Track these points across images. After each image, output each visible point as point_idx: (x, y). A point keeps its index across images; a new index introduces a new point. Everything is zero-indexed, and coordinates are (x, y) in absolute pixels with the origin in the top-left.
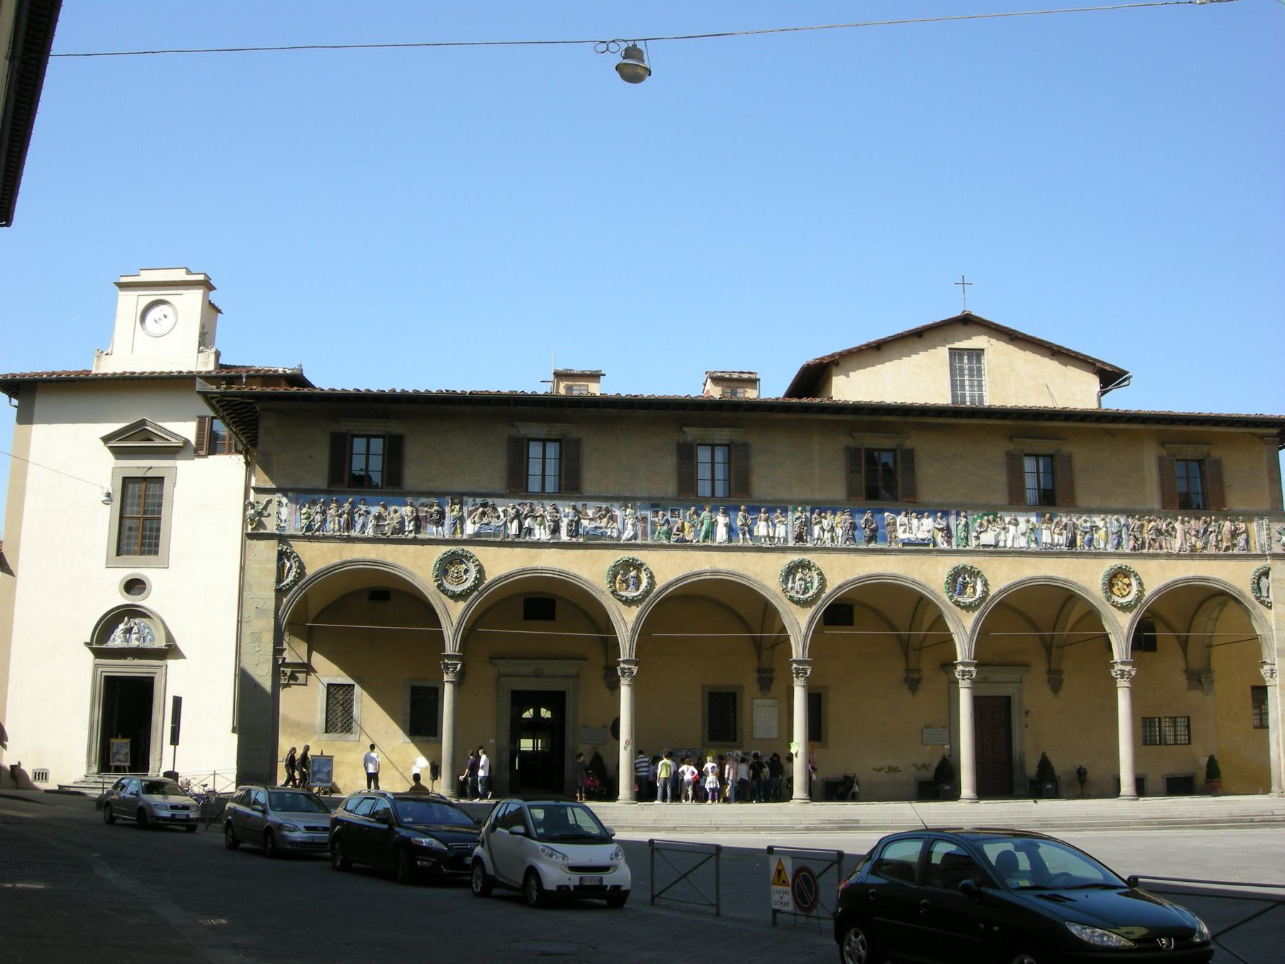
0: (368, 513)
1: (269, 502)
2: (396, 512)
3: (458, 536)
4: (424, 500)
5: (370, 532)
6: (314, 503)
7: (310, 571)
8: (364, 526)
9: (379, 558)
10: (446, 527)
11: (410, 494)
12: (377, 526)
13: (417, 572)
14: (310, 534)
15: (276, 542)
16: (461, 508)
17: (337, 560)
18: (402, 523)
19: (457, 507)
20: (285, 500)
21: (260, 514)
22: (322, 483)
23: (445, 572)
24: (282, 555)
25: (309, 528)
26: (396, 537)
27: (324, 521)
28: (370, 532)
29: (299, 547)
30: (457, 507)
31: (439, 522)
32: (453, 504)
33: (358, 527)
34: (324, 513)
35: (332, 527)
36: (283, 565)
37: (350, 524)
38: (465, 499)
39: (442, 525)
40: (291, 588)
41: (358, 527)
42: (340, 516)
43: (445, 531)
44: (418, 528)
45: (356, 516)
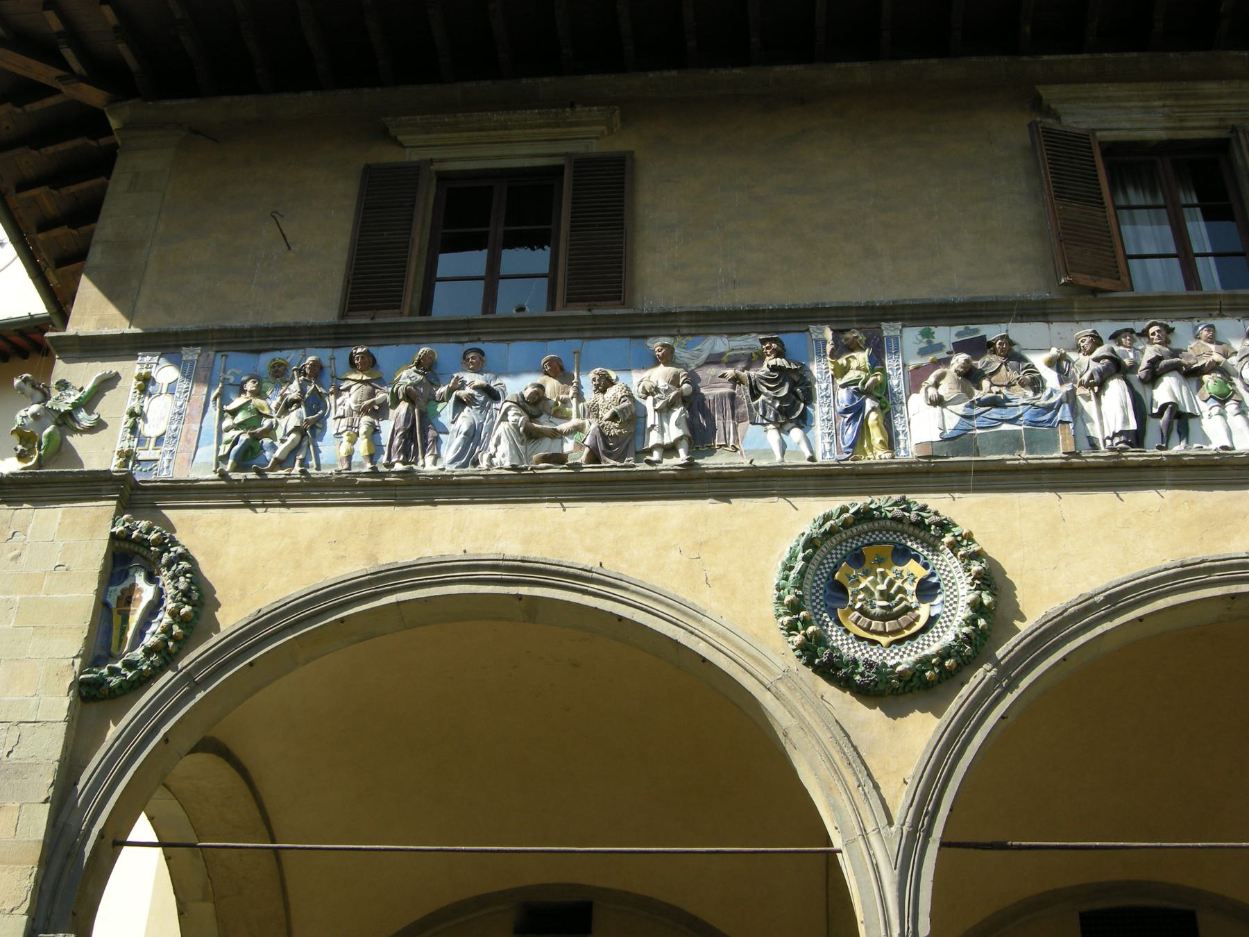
0: (492, 394)
1: (108, 383)
2: (604, 384)
3: (877, 454)
4: (721, 344)
5: (500, 453)
6: (280, 374)
7: (231, 617)
8: (473, 437)
9: (539, 552)
10: (819, 429)
11: (664, 321)
12: (530, 435)
13: (706, 599)
14: (252, 480)
15: (108, 507)
16: (877, 361)
17: (354, 567)
18: (631, 418)
19: (861, 358)
20: (166, 373)
21: (66, 421)
22: (322, 309)
23: (837, 592)
24: (124, 558)
25: (248, 455)
26: (614, 471)
27: (311, 432)
28: (500, 453)
29: (196, 529)
30: (861, 358)
31: (793, 409)
32: (843, 347)
33: (450, 446)
34: (315, 404)
35: (336, 450)
36: (127, 599)
37: (418, 435)
38: (889, 330)
39: (804, 422)
40: (143, 681)
41: (450, 446)
42: (379, 412)
43: (819, 443)
44: (700, 437)
45: (445, 412)
